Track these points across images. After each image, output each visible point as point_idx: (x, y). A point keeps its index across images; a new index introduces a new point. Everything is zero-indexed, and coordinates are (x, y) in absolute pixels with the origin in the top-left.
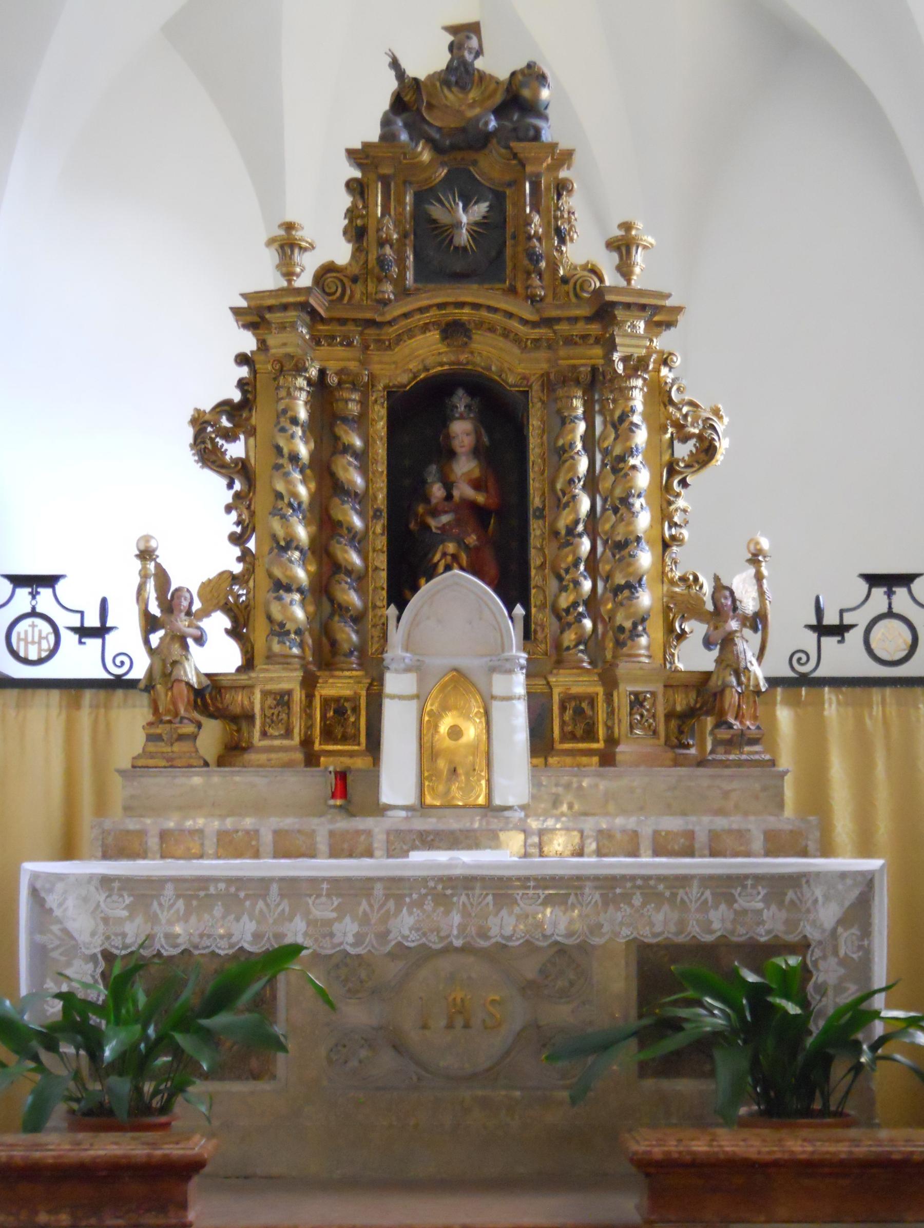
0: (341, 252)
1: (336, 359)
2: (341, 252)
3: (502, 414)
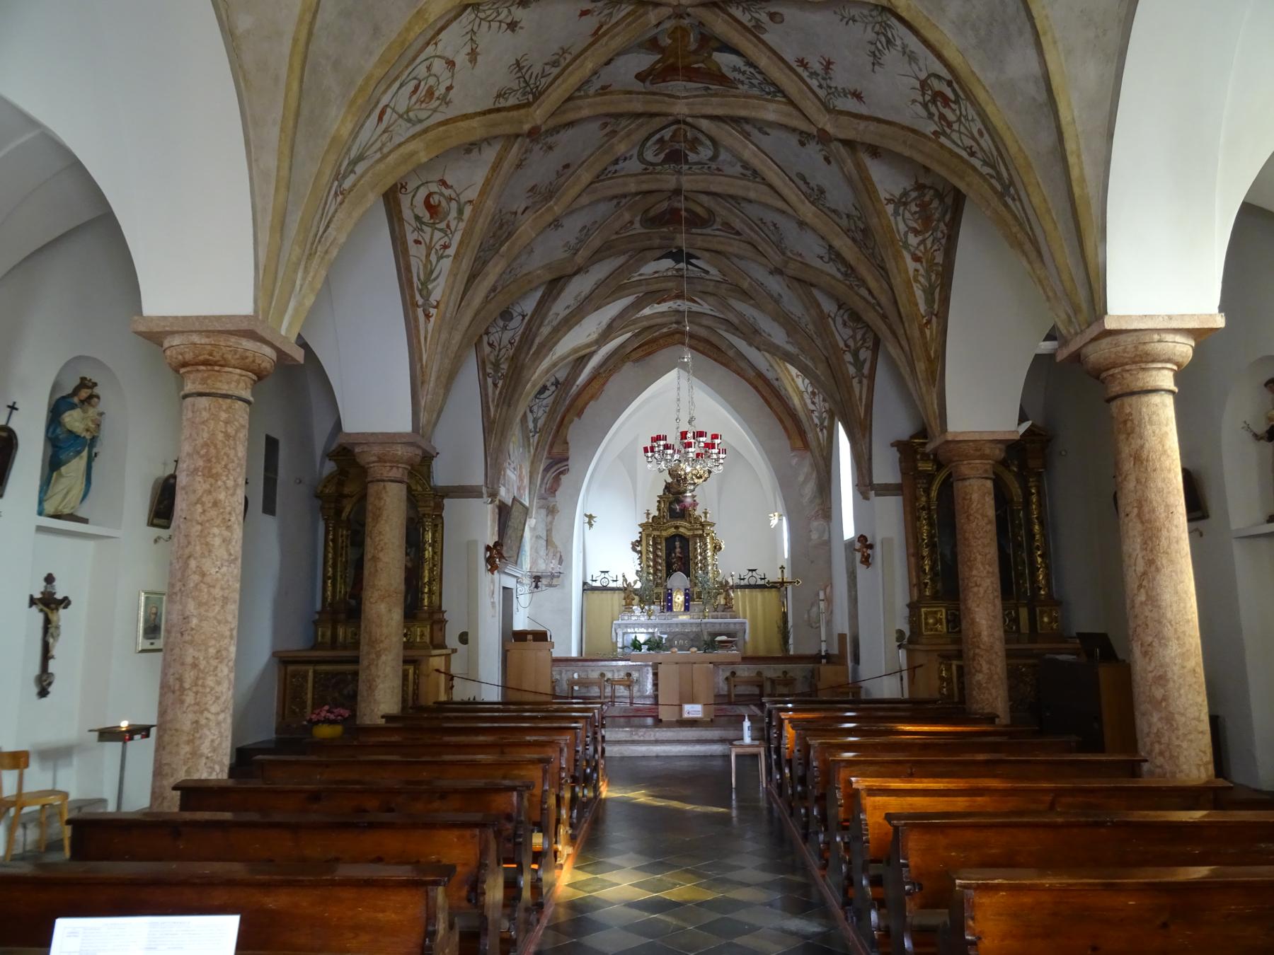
0: (656, 513)
1: (656, 533)
2: (656, 513)
3: (684, 540)
